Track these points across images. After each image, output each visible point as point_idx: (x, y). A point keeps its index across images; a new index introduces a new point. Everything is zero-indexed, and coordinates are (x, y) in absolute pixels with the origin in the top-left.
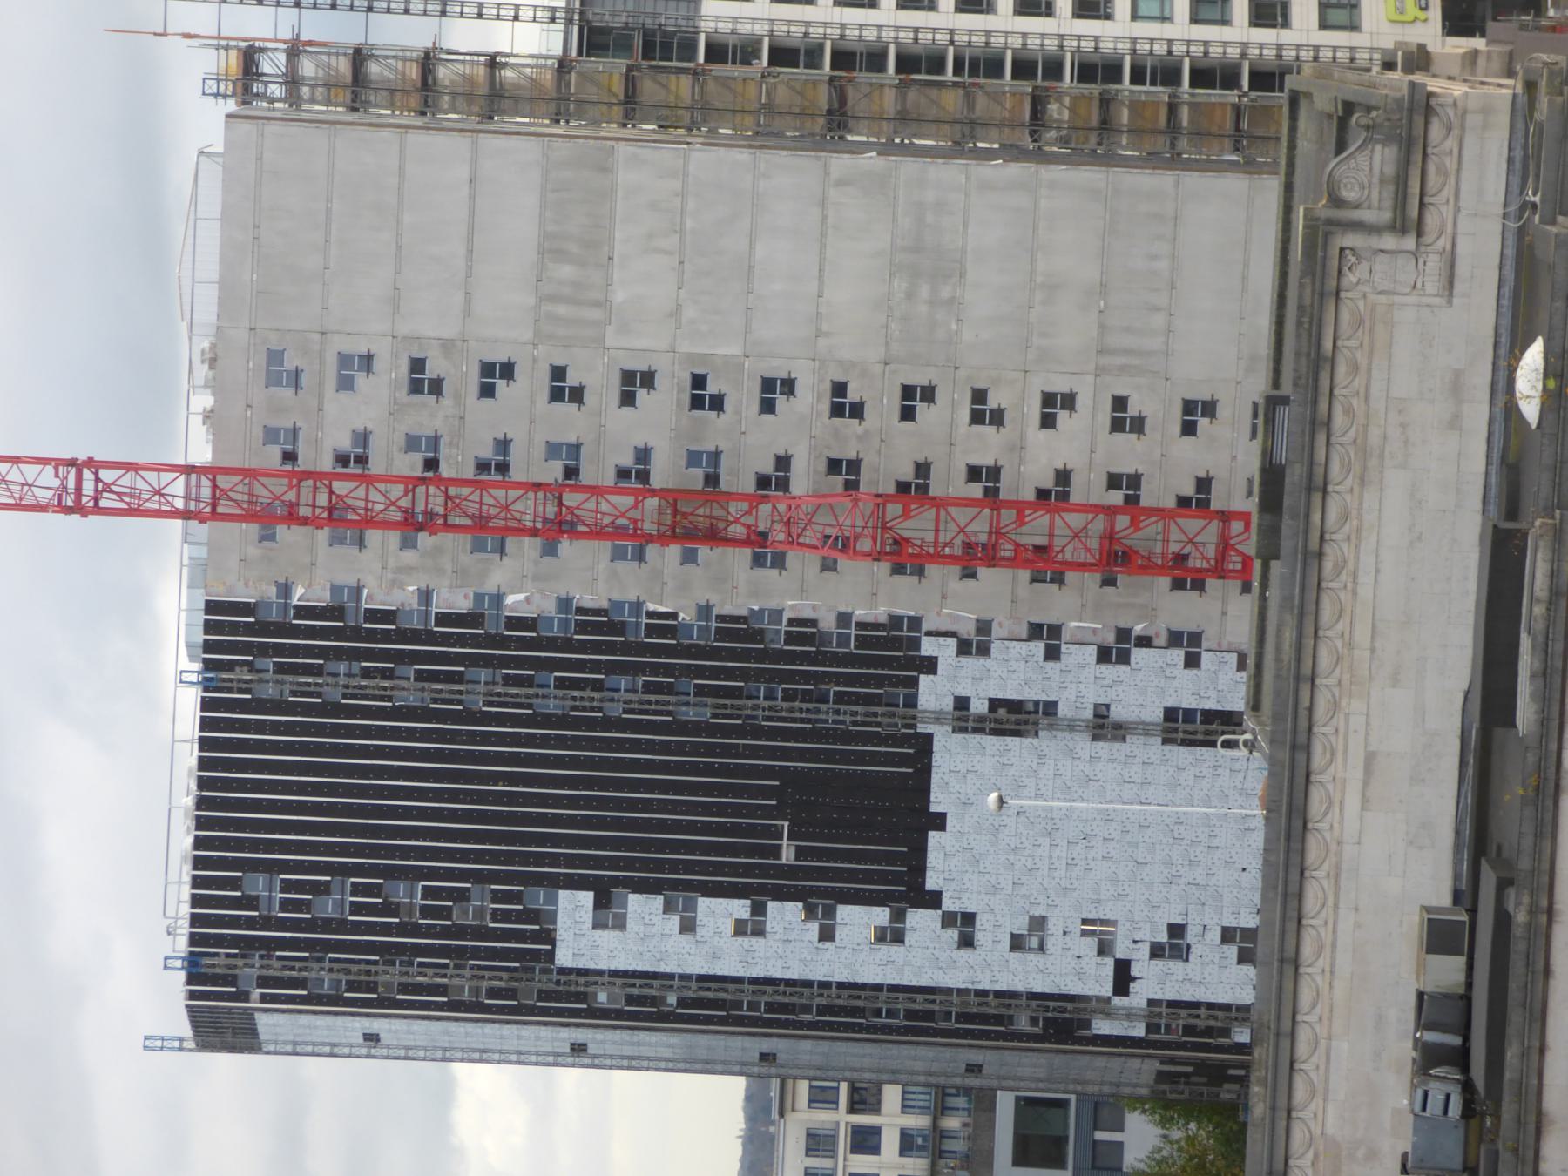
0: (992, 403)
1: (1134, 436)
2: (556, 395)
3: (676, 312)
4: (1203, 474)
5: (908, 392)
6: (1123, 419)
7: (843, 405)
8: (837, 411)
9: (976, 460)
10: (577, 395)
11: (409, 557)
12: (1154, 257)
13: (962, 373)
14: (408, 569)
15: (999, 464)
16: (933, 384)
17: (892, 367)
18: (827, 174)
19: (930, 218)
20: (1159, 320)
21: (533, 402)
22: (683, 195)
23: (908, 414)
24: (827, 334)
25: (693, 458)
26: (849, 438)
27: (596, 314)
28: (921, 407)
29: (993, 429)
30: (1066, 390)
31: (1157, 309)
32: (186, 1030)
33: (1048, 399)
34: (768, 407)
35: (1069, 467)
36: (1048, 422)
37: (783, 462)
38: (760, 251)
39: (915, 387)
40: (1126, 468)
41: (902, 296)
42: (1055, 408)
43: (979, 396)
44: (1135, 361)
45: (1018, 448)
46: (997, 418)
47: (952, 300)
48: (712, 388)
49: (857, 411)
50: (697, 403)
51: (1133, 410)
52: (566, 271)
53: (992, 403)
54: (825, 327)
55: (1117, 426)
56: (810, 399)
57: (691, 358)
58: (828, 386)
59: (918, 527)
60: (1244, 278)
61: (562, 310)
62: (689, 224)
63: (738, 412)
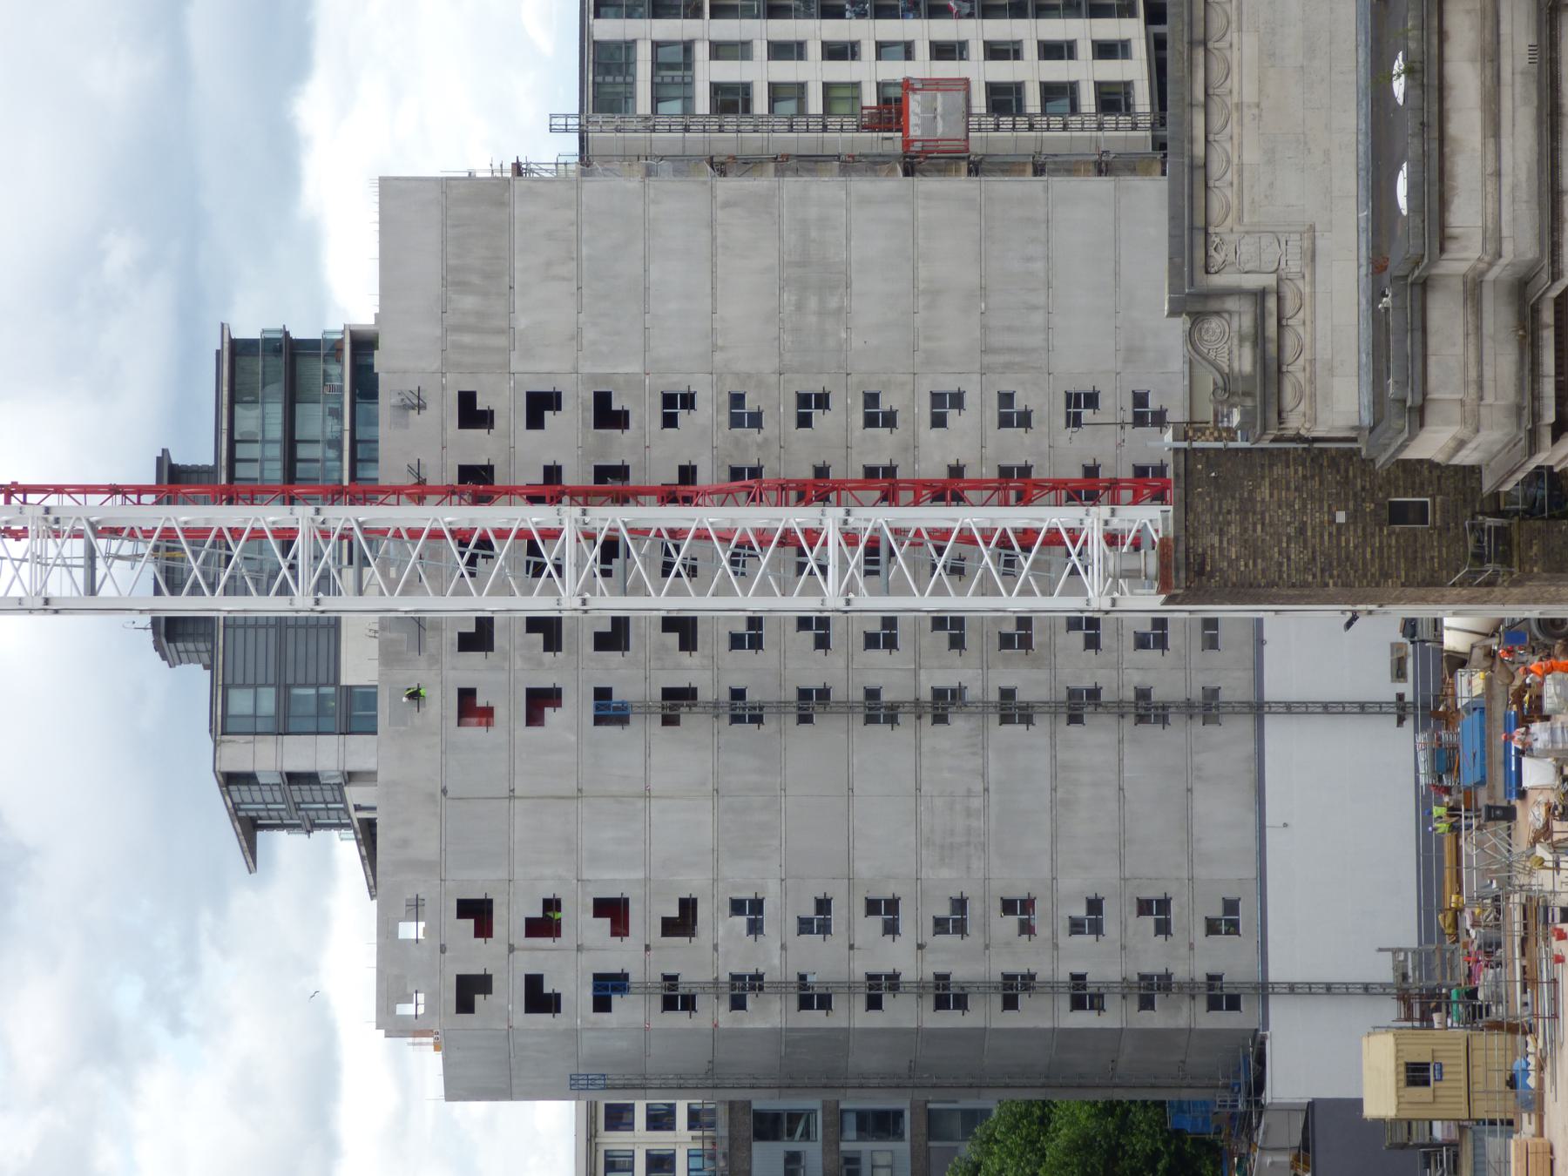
0: (884, 406)
1: (1022, 430)
3: (577, 336)
4: (1090, 463)
5: (804, 400)
6: (1012, 416)
7: (741, 414)
8: (736, 421)
12: (1030, 259)
13: (853, 379)
15: (894, 463)
16: (827, 390)
17: (787, 376)
18: (713, 197)
19: (814, 234)
20: (1038, 318)
21: (443, 429)
22: (578, 224)
23: (804, 421)
24: (722, 349)
27: (501, 341)
28: (816, 414)
29: (887, 430)
30: (955, 390)
31: (1035, 308)
33: (937, 399)
34: (670, 421)
35: (961, 463)
36: (939, 421)
38: (654, 274)
39: (809, 395)
40: (1016, 460)
41: (793, 308)
42: (945, 408)
43: (872, 399)
44: (1017, 359)
45: (913, 447)
46: (890, 420)
47: (840, 310)
49: (756, 420)
51: (1019, 406)
52: (469, 302)
53: (884, 406)
54: (720, 342)
55: (1005, 421)
56: (708, 413)
57: (593, 377)
58: (726, 397)
60: (1116, 274)
61: (467, 339)
62: (585, 251)
63: (641, 427)
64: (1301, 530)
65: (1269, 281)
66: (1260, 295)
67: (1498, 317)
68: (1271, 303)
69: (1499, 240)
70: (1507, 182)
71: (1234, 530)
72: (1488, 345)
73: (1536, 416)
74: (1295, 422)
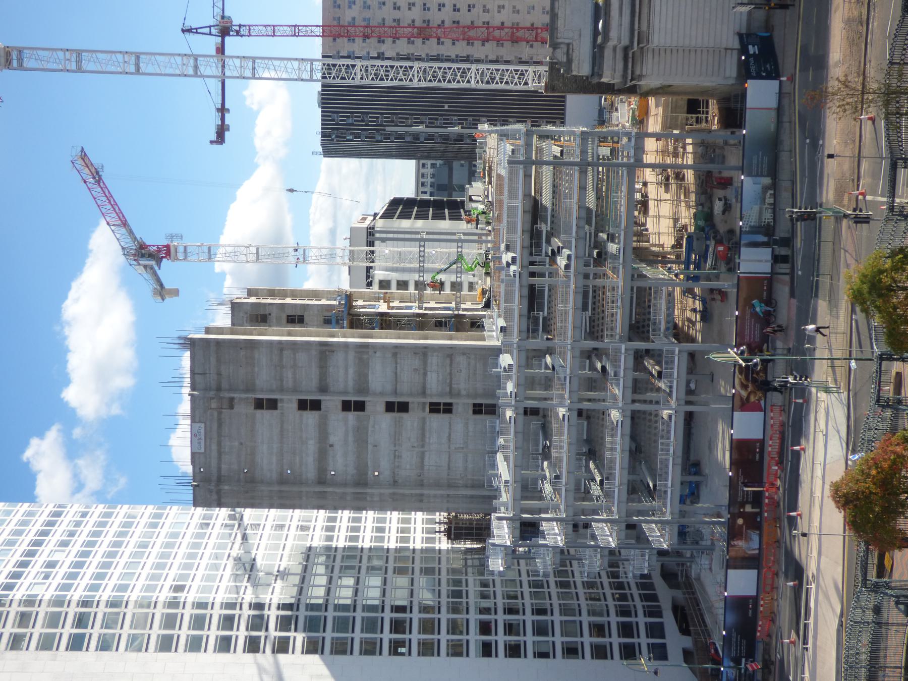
2: (395, 8)
5: (469, 6)
7: (456, 9)
8: (454, 10)
9: (484, 20)
10: (399, 8)
11: (364, 45)
14: (363, 47)
23: (469, 11)
25: (424, 21)
26: (457, 16)
32: (320, 149)
34: (439, 10)
36: (499, 12)
37: (443, 22)
43: (484, 6)
48: (427, 6)
49: (459, 10)
50: (424, 9)
56: (448, 8)
59: (472, 33)
64: (576, 81)
65: (570, 41)
66: (568, 45)
67: (620, 55)
68: (571, 46)
69: (620, 40)
70: (623, 27)
71: (561, 80)
72: (617, 61)
73: (627, 78)
74: (574, 73)
